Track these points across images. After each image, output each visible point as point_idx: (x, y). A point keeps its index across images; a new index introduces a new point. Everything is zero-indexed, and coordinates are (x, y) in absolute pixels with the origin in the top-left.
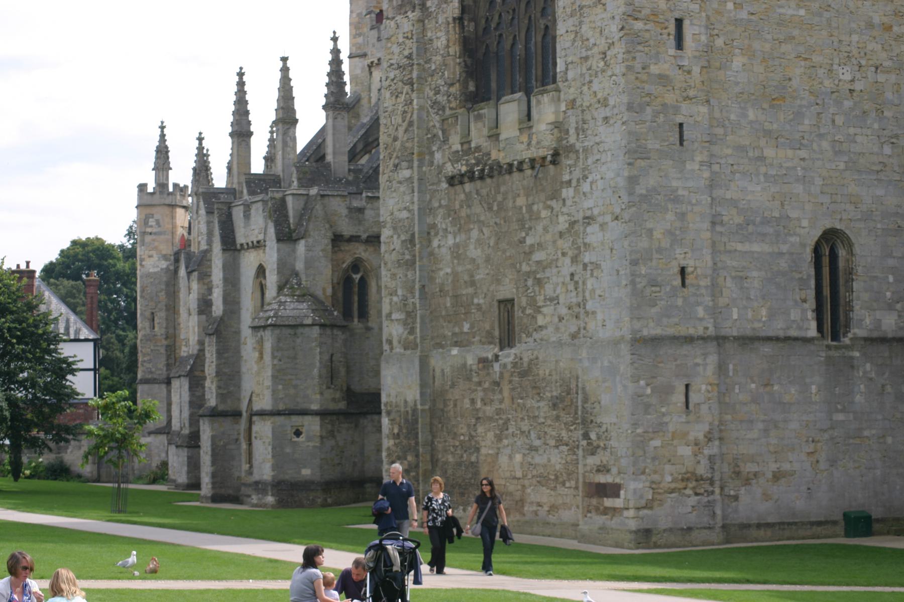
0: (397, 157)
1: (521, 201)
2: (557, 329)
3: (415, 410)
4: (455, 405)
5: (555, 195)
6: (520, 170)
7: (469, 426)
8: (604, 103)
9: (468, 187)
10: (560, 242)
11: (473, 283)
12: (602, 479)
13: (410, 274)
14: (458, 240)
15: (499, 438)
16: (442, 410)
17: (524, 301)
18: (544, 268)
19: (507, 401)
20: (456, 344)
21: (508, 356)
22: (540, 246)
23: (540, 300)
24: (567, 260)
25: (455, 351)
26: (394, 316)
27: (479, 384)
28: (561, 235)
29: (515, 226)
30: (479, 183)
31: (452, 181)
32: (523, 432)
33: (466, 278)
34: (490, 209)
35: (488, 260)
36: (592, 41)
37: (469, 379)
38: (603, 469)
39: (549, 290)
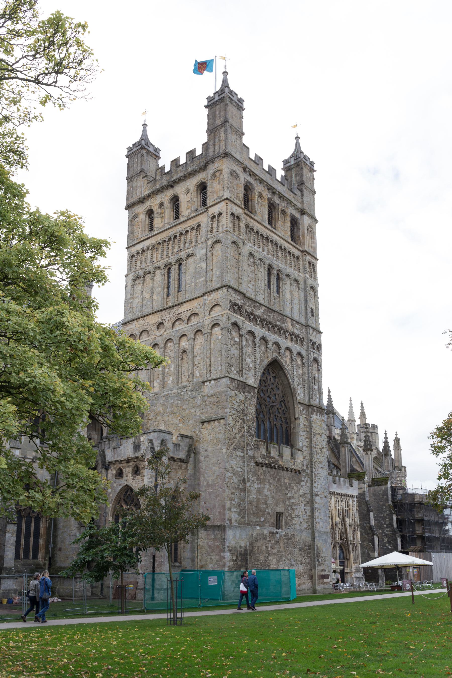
0: (235, 445)
1: (287, 481)
2: (300, 526)
3: (245, 550)
4: (258, 549)
5: (299, 483)
6: (287, 471)
7: (264, 557)
9: (264, 469)
10: (300, 498)
11: (266, 504)
12: (323, 573)
13: (242, 494)
14: (259, 486)
15: (279, 561)
16: (252, 550)
17: (287, 514)
18: (295, 505)
19: (282, 548)
20: (258, 525)
21: (282, 532)
22: (293, 498)
23: (293, 515)
24: (303, 505)
25: (258, 528)
26: (232, 510)
27: (270, 541)
28: (301, 496)
29: (284, 488)
30: (269, 469)
31: (257, 464)
32: (288, 559)
33: (263, 501)
34: (274, 479)
35: (273, 497)
36: (317, 444)
37: (265, 539)
38: (323, 570)
39: (296, 512)
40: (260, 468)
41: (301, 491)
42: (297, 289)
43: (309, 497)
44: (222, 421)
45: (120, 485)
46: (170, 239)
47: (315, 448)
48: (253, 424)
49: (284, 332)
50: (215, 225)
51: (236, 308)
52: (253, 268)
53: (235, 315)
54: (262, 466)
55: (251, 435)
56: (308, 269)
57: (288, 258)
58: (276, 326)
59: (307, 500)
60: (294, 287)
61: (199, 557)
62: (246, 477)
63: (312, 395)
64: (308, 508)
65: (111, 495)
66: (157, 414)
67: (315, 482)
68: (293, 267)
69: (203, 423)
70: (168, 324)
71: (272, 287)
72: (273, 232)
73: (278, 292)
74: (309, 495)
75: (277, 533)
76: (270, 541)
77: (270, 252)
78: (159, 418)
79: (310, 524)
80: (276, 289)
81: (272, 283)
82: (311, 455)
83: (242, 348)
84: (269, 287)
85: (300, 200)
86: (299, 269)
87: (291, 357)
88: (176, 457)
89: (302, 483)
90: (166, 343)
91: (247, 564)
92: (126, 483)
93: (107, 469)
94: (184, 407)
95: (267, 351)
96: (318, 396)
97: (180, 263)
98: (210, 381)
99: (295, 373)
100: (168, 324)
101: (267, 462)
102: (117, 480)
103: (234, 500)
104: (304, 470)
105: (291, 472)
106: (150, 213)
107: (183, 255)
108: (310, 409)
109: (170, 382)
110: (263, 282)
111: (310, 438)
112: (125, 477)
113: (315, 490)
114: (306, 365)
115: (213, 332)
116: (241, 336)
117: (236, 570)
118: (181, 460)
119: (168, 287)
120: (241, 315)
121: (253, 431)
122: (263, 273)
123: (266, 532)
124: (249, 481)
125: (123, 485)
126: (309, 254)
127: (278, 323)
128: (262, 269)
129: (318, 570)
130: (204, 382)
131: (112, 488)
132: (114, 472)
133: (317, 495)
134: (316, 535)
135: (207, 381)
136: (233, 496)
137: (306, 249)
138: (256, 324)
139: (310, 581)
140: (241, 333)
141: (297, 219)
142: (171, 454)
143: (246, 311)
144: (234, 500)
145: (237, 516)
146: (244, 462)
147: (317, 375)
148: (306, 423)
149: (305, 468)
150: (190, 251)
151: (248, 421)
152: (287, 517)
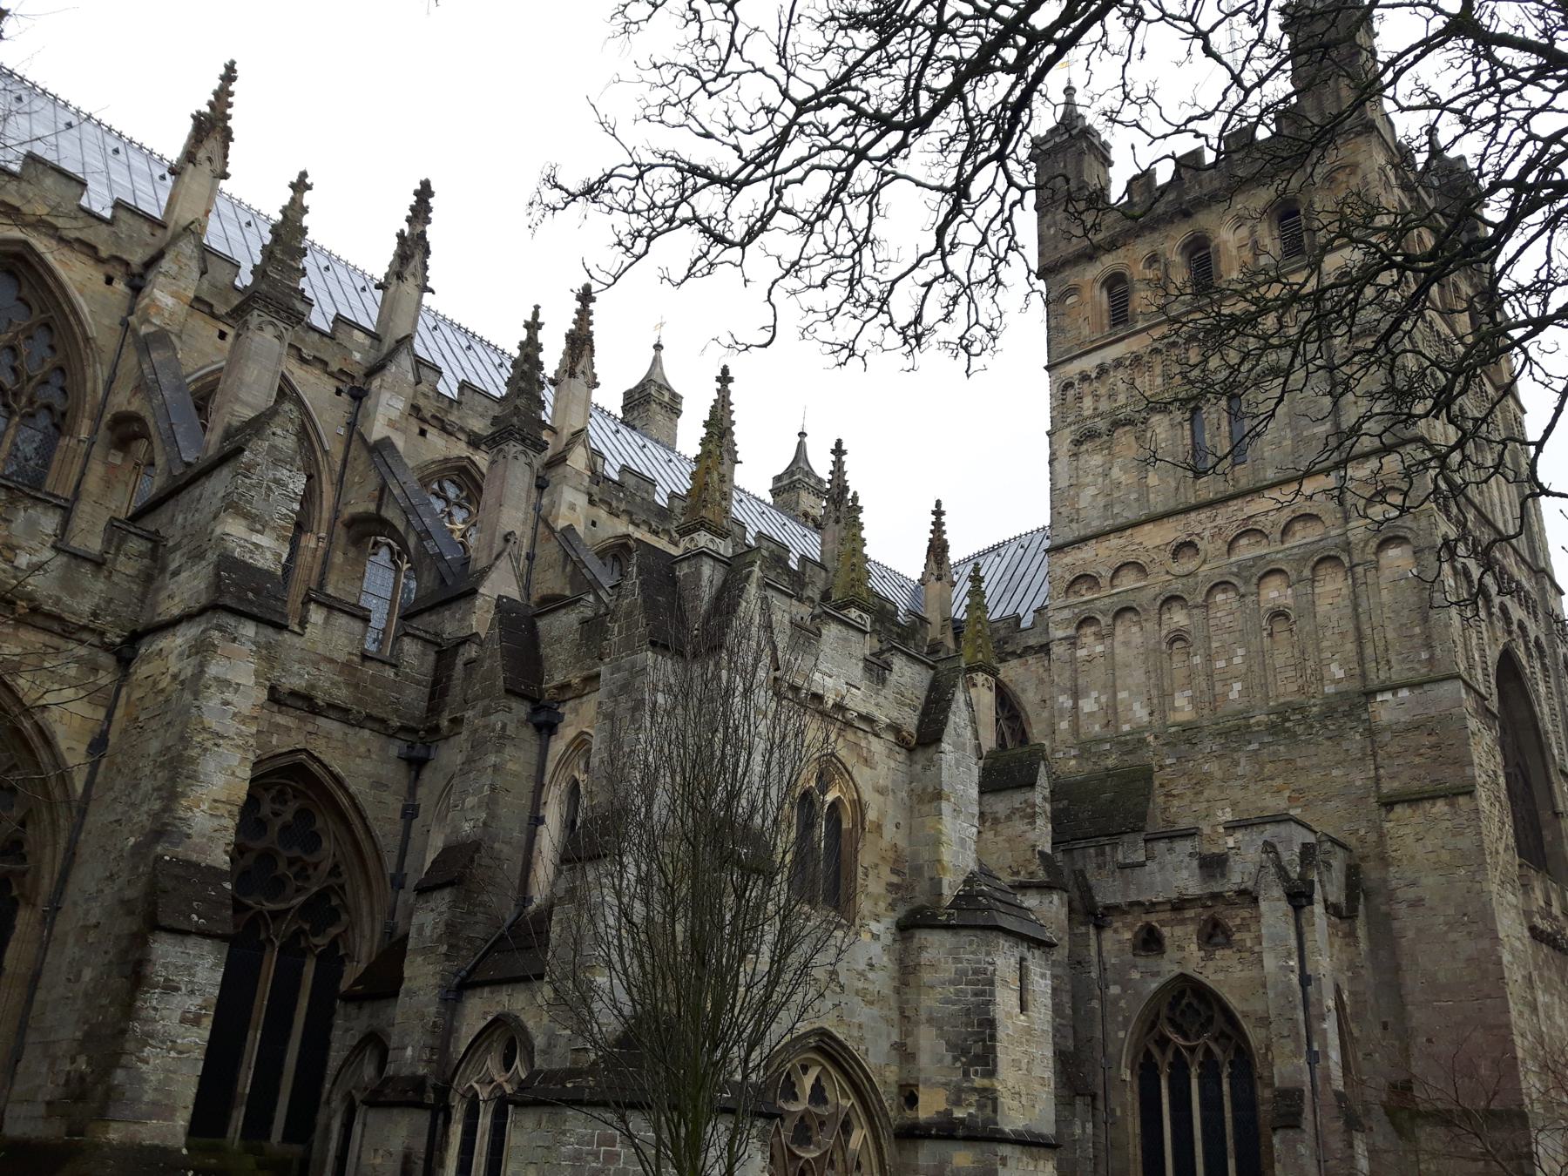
44: (1462, 800)
45: (1156, 974)
65: (1122, 1004)
66: (1200, 784)
69: (1388, 804)
90: (1210, 592)
92: (1177, 970)
93: (1100, 928)
98: (1394, 688)
102: (1140, 961)
109: (1234, 695)
112: (1171, 953)
115: (1382, 562)
125: (1168, 977)
131: (1125, 984)
132: (1128, 935)
135: (1383, 690)
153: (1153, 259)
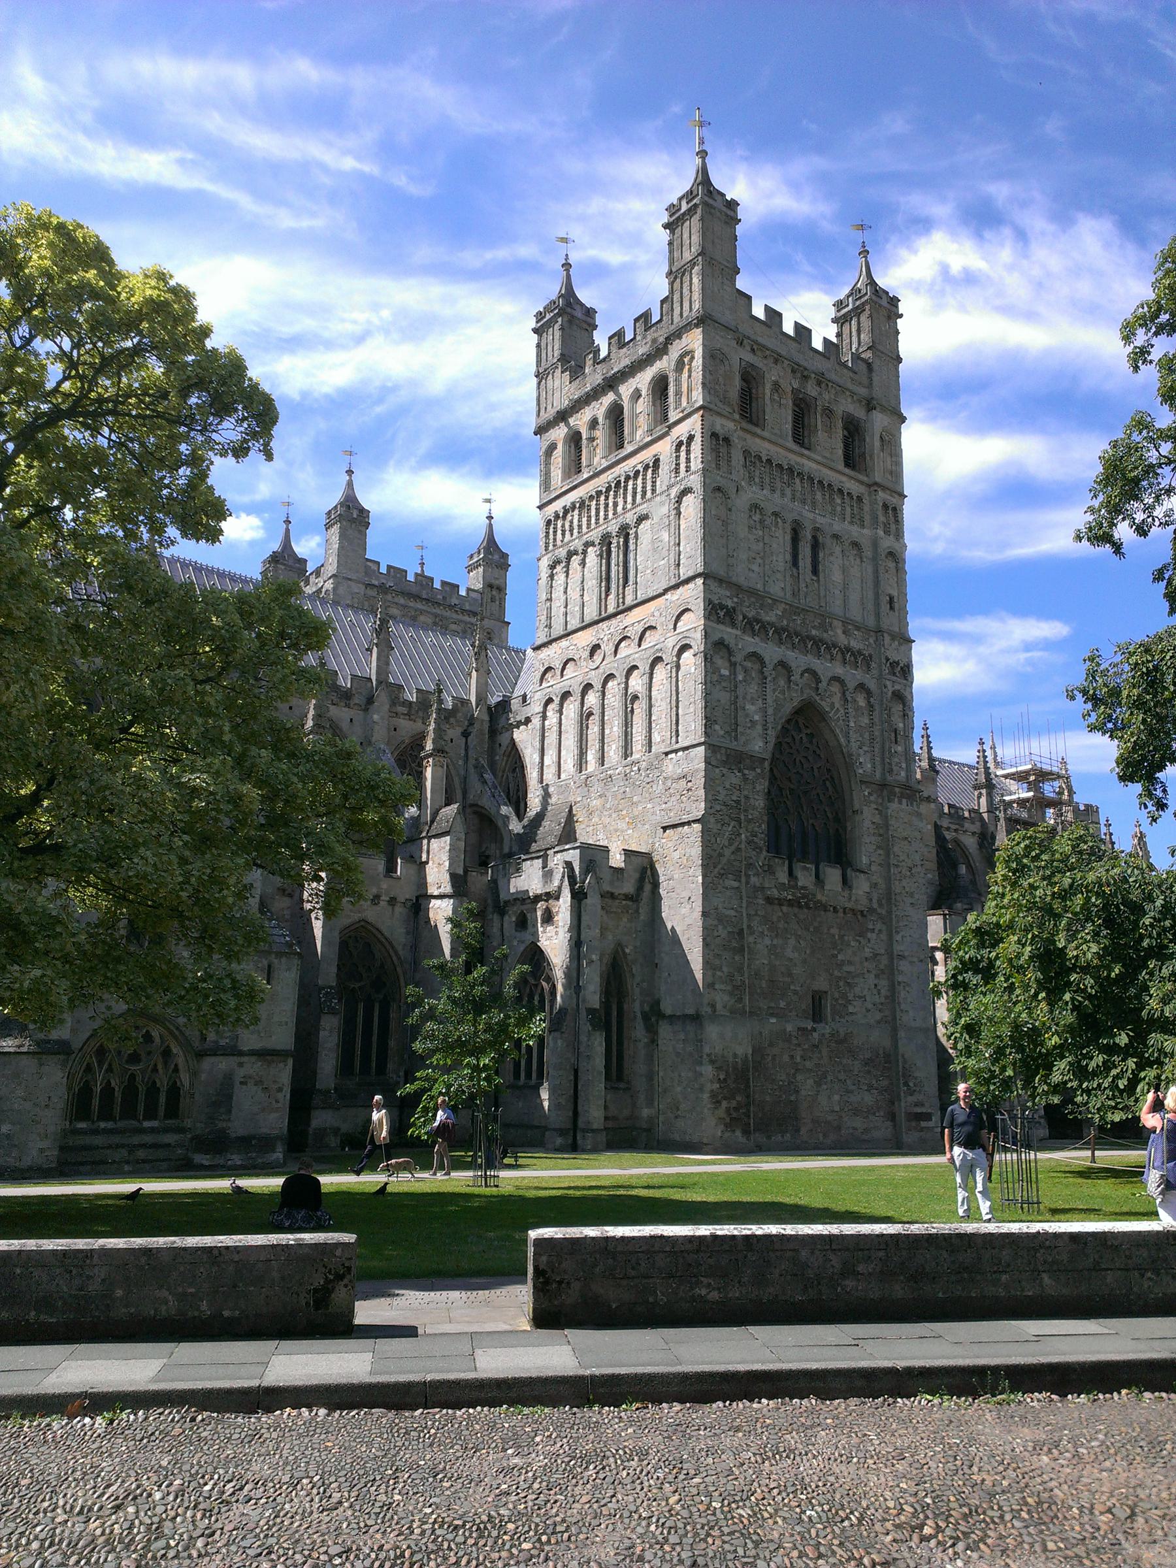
1: (834, 931)
7: (788, 1074)
8: (912, 895)
9: (785, 908)
10: (866, 964)
11: (790, 975)
12: (919, 1110)
13: (737, 958)
14: (775, 942)
17: (836, 995)
18: (853, 978)
20: (772, 1015)
21: (826, 1029)
22: (850, 963)
25: (773, 1020)
26: (717, 986)
30: (796, 910)
31: (769, 900)
35: (805, 961)
36: (902, 858)
39: (857, 990)
40: (776, 908)
41: (867, 950)
42: (858, 560)
43: (884, 961)
45: (523, 942)
46: (608, 489)
47: (897, 866)
48: (760, 826)
49: (828, 648)
50: (683, 454)
51: (722, 614)
52: (761, 533)
53: (721, 627)
54: (781, 905)
55: (758, 849)
56: (882, 518)
57: (839, 501)
58: (810, 638)
59: (882, 967)
60: (851, 558)
61: (661, 1074)
62: (745, 927)
63: (890, 764)
64: (884, 983)
67: (897, 932)
68: (848, 518)
69: (665, 828)
70: (607, 648)
71: (801, 564)
72: (802, 455)
73: (815, 571)
74: (885, 957)
75: (814, 1030)
76: (799, 1045)
77: (798, 494)
78: (595, 820)
79: (887, 1013)
80: (809, 566)
81: (800, 557)
82: (888, 880)
83: (736, 687)
84: (795, 563)
85: (865, 381)
86: (862, 520)
87: (844, 694)
88: (616, 892)
89: (869, 935)
91: (748, 1086)
94: (635, 799)
95: (789, 687)
96: (904, 765)
97: (624, 531)
99: (852, 724)
100: (607, 648)
101: (790, 897)
102: (518, 934)
103: (720, 969)
104: (872, 910)
105: (844, 913)
106: (575, 439)
107: (630, 518)
108: (885, 793)
109: (612, 753)
110: (781, 556)
111: (886, 846)
113: (897, 948)
114: (877, 707)
116: (733, 665)
117: (725, 1098)
118: (627, 897)
119: (608, 579)
120: (733, 625)
121: (761, 840)
122: (781, 538)
123: (789, 1028)
124: (752, 933)
125: (528, 943)
126: (884, 488)
127: (814, 632)
128: (779, 533)
129: (906, 1103)
130: (667, 754)
132: (514, 919)
133: (901, 957)
134: (902, 1034)
136: (717, 962)
137: (878, 480)
138: (766, 639)
139: (889, 1123)
140: (733, 659)
141: (859, 420)
142: (606, 887)
143: (744, 617)
144: (720, 969)
145: (726, 998)
146: (741, 898)
147: (901, 725)
148: (877, 819)
149: (875, 906)
150: (642, 509)
151: (749, 821)
152: (837, 1000)
153: (594, 423)
